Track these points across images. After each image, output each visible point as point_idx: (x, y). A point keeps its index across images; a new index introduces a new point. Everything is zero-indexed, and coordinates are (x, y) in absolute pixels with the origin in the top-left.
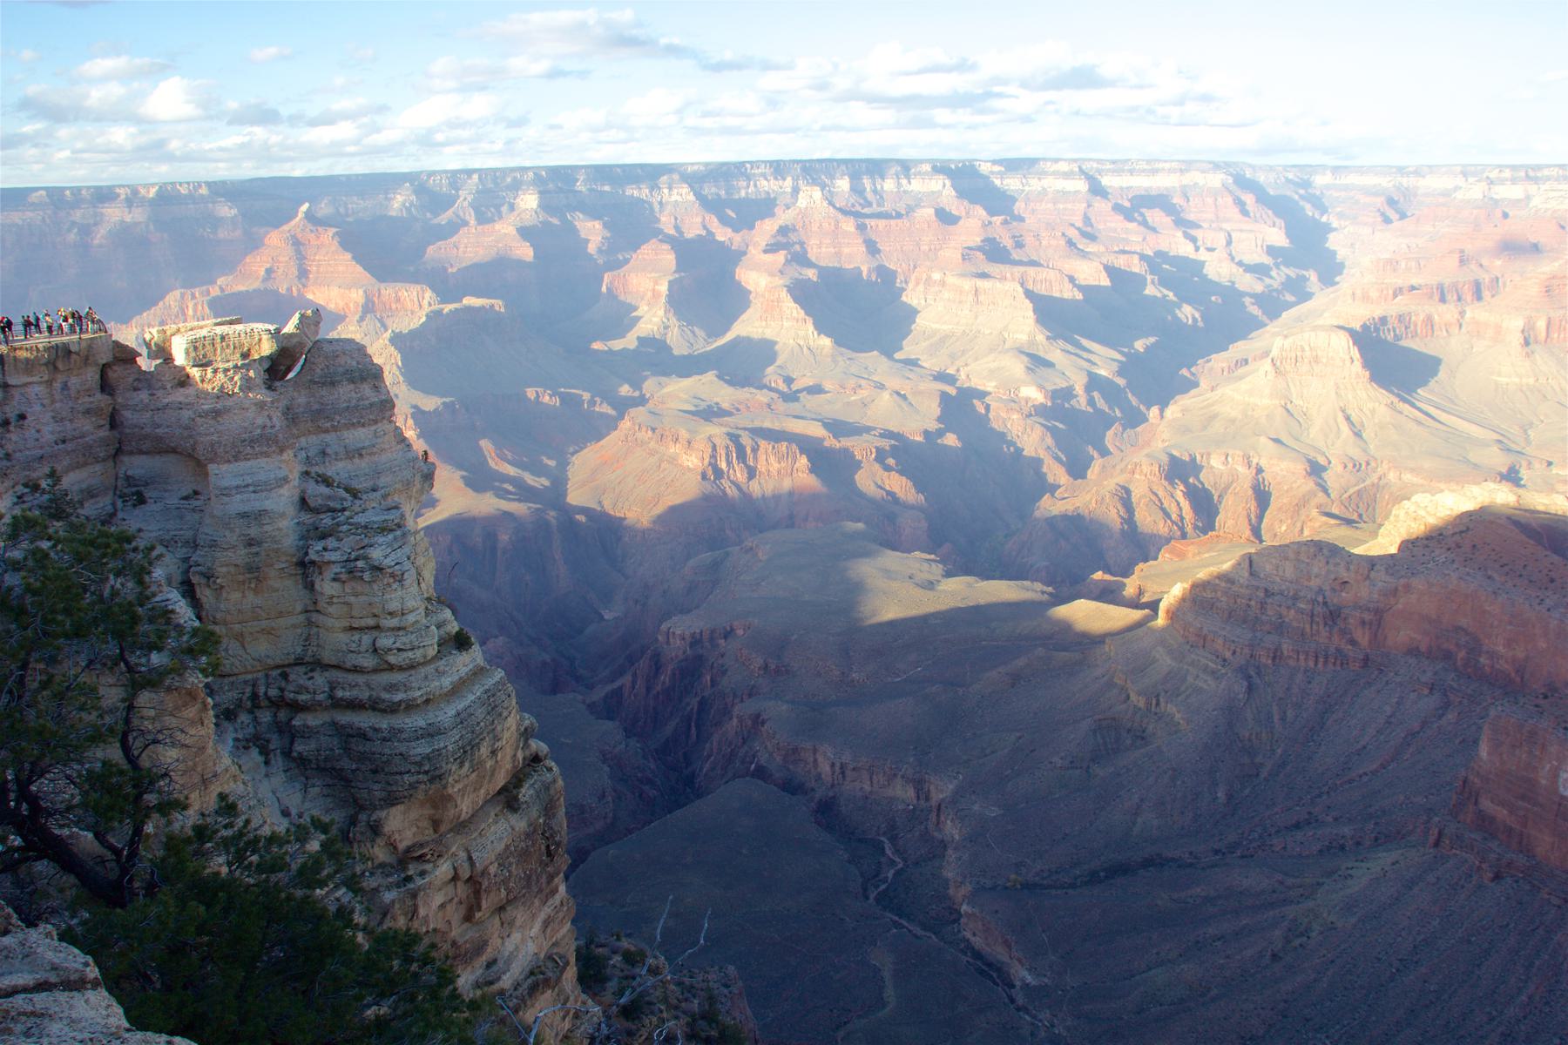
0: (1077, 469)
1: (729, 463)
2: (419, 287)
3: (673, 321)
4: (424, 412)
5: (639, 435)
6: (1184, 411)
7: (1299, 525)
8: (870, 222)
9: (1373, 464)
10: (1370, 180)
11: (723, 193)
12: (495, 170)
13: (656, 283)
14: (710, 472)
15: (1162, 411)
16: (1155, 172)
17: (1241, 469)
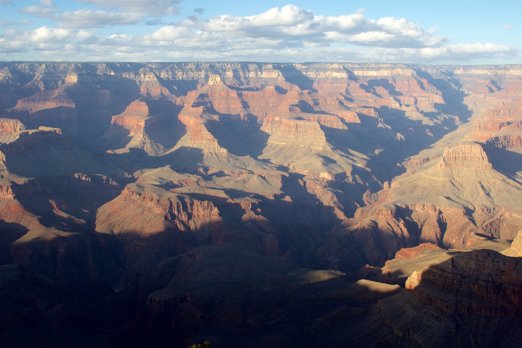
0: (350, 213)
1: (179, 211)
2: (14, 120)
3: (148, 140)
4: (18, 185)
5: (133, 197)
6: (401, 184)
7: (462, 240)
8: (245, 93)
9: (497, 209)
10: (480, 72)
11: (170, 77)
12: (54, 63)
13: (139, 121)
14: (169, 216)
15: (389, 184)
16: (379, 69)
17: (431, 212)
